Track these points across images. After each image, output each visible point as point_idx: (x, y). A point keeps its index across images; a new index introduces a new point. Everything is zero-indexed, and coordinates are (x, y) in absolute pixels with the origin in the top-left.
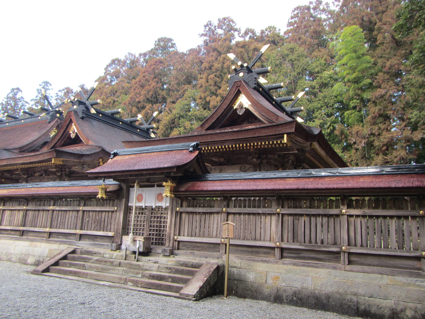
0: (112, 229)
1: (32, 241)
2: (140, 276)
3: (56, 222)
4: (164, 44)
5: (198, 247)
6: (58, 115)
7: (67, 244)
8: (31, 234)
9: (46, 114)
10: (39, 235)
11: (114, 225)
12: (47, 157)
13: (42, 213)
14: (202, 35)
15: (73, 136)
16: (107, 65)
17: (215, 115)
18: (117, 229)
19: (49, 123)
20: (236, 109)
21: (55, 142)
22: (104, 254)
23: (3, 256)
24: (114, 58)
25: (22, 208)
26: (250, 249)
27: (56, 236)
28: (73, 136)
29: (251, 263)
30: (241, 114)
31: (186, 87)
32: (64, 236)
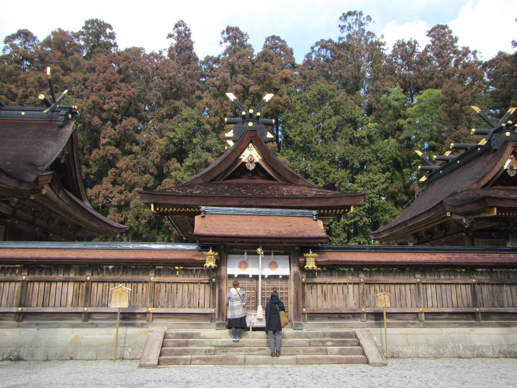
1: (508, 326)
4: (97, 32)
6: (70, 116)
8: (493, 317)
9: (50, 110)
12: (347, 203)
14: (170, 36)
15: (251, 167)
16: (9, 37)
19: (61, 127)
20: (507, 169)
21: (219, 173)
23: (461, 351)
24: (22, 28)
25: (469, 282)
28: (251, 167)
31: (178, 103)
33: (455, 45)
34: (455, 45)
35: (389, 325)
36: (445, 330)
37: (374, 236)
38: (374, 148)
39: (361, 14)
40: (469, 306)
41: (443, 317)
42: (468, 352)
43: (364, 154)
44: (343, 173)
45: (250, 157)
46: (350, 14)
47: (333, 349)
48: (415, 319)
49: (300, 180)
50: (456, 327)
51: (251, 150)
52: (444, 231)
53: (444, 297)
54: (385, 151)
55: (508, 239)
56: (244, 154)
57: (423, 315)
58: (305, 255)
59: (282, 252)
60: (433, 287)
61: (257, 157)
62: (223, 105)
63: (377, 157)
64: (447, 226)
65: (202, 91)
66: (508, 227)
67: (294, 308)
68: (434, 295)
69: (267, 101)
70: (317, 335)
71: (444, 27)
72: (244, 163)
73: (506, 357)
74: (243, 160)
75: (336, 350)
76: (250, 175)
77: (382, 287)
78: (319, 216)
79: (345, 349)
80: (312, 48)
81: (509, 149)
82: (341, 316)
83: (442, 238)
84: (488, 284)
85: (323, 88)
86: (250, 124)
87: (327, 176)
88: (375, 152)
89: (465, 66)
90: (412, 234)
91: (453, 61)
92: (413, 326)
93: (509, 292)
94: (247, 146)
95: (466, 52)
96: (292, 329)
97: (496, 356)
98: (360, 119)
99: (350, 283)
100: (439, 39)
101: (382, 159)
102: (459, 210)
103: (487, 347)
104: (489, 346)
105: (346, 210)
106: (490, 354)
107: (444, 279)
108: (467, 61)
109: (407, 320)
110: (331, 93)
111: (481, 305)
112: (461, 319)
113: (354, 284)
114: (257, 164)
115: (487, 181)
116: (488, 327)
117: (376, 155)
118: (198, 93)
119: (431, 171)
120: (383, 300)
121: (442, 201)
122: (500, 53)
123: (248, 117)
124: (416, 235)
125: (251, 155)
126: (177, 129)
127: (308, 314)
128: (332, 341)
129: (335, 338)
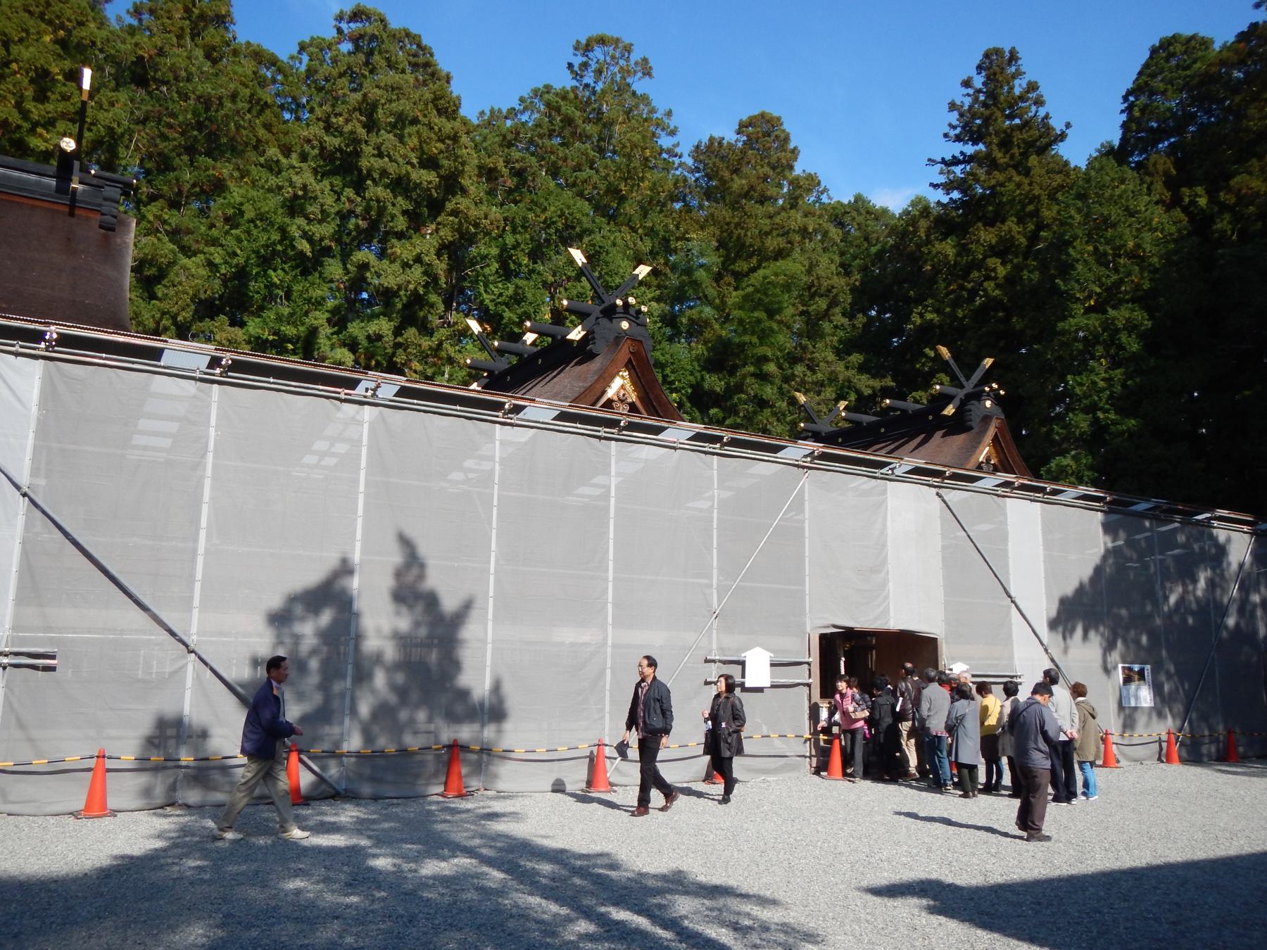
31: (225, 169)
38: (662, 358)
39: (628, 49)
45: (622, 392)
46: (602, 41)
62: (343, 199)
65: (287, 151)
80: (522, 100)
81: (991, 432)
85: (569, 207)
86: (625, 325)
101: (672, 383)
118: (273, 152)
122: (858, 198)
123: (632, 311)
126: (230, 242)
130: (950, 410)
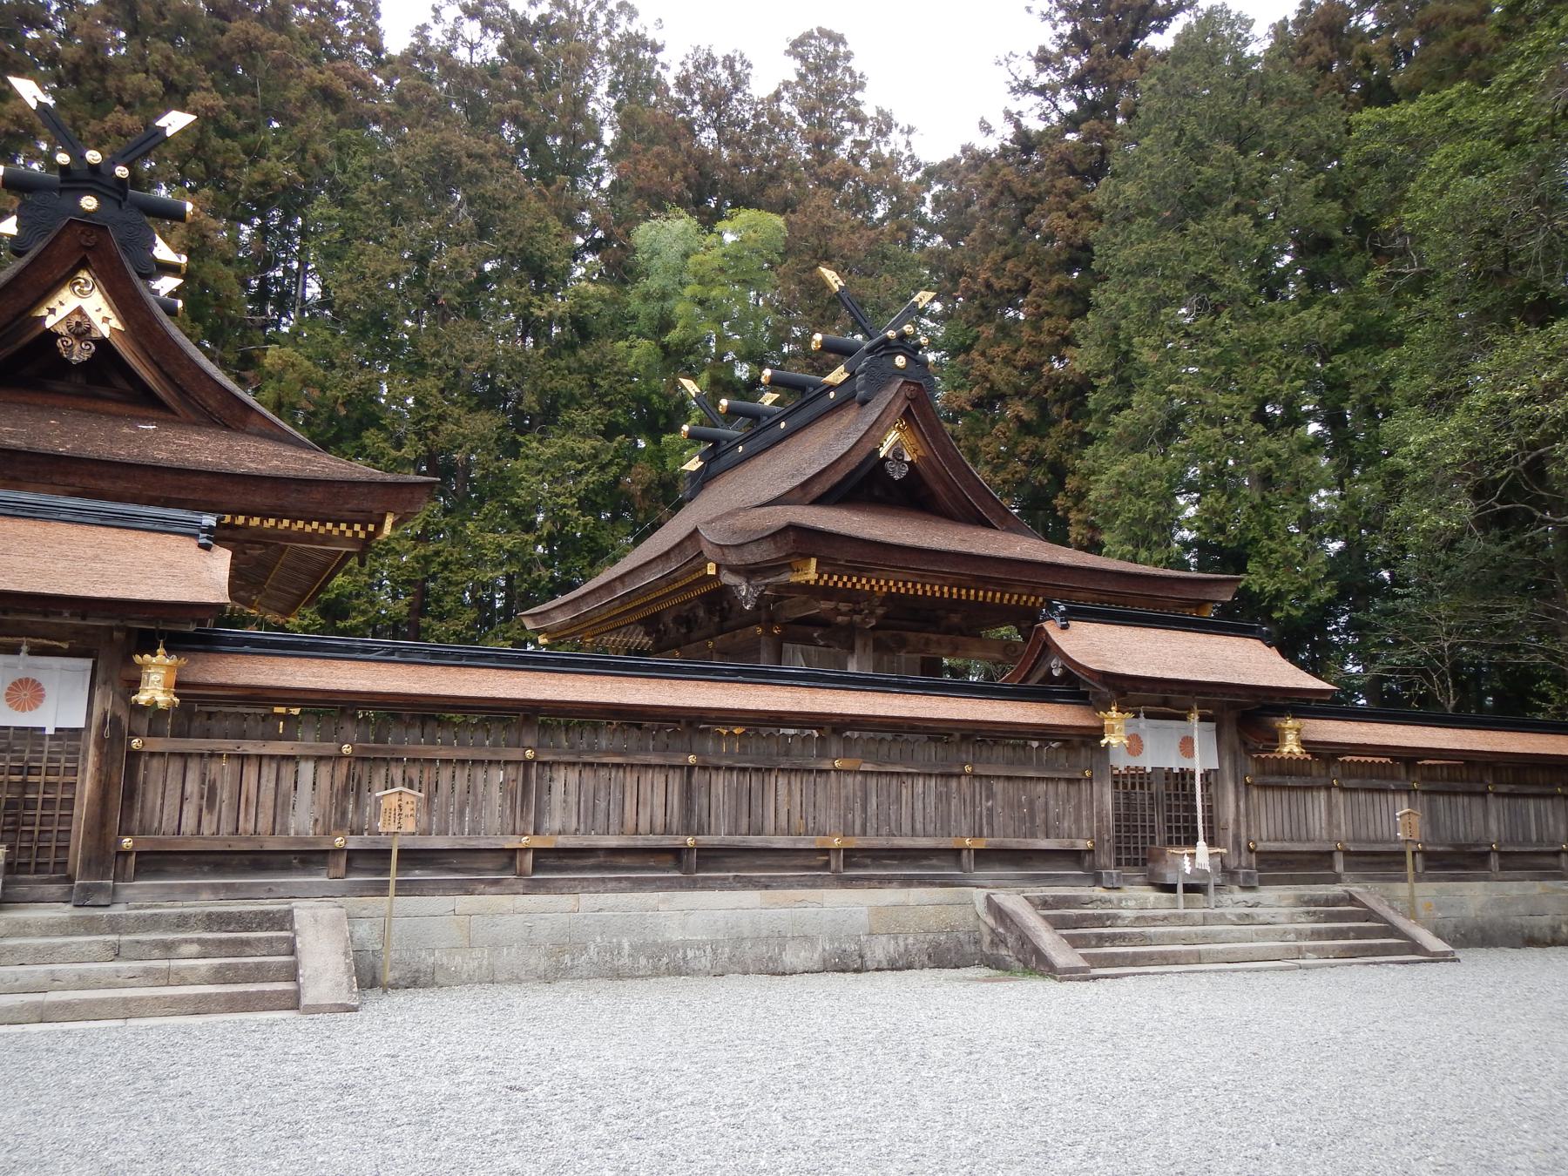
0: (1086, 833)
1: (767, 887)
2: (1292, 937)
3: (858, 813)
5: (1291, 862)
7: (932, 885)
8: (731, 862)
10: (784, 862)
11: (1090, 819)
13: (783, 781)
15: (80, 353)
17: (843, 464)
18: (1099, 832)
20: (885, 459)
22: (1120, 901)
23: (626, 960)
25: (679, 761)
26: (1376, 859)
27: (868, 861)
28: (80, 353)
29: (1392, 885)
30: (896, 477)
32: (902, 858)
33: (858, 95)
34: (858, 95)
35: (405, 889)
36: (588, 900)
37: (535, 621)
38: (587, 360)
40: (667, 831)
41: (591, 861)
42: (643, 961)
43: (557, 370)
44: (485, 423)
45: (77, 318)
47: (192, 968)
48: (502, 870)
49: (254, 417)
50: (623, 891)
51: (82, 294)
52: (717, 619)
53: (602, 805)
54: (617, 373)
55: (851, 650)
56: (53, 304)
57: (530, 856)
58: (137, 659)
59: (65, 646)
60: (573, 776)
61: (106, 320)
63: (594, 385)
64: (725, 605)
66: (857, 618)
67: (88, 833)
68: (573, 799)
69: (169, 133)
70: (154, 923)
71: (838, 40)
72: (52, 335)
73: (746, 973)
74: (50, 322)
75: (203, 970)
76: (80, 380)
77: (414, 772)
78: (218, 536)
79: (235, 967)
82: (260, 861)
83: (710, 637)
84: (730, 769)
86: (89, 203)
87: (434, 429)
88: (592, 371)
89: (878, 162)
90: (640, 622)
91: (847, 142)
92: (493, 889)
93: (783, 791)
94: (66, 278)
95: (885, 124)
96: (69, 907)
97: (719, 971)
98: (557, 265)
99: (307, 758)
100: (817, 70)
101: (606, 394)
102: (733, 559)
103: (700, 946)
104: (705, 944)
105: (371, 528)
106: (705, 963)
107: (607, 753)
108: (886, 151)
109: (479, 871)
110: (471, 165)
111: (701, 827)
112: (643, 869)
113: (319, 759)
114: (102, 343)
115: (828, 486)
116: (713, 889)
117: (590, 380)
119: (716, 442)
120: (397, 811)
121: (696, 530)
124: (651, 624)
125: (79, 311)
127: (139, 854)
128: (200, 942)
129: (219, 930)
130: (838, 376)
